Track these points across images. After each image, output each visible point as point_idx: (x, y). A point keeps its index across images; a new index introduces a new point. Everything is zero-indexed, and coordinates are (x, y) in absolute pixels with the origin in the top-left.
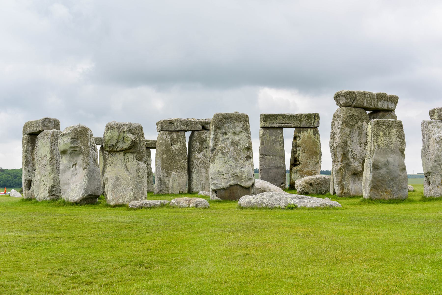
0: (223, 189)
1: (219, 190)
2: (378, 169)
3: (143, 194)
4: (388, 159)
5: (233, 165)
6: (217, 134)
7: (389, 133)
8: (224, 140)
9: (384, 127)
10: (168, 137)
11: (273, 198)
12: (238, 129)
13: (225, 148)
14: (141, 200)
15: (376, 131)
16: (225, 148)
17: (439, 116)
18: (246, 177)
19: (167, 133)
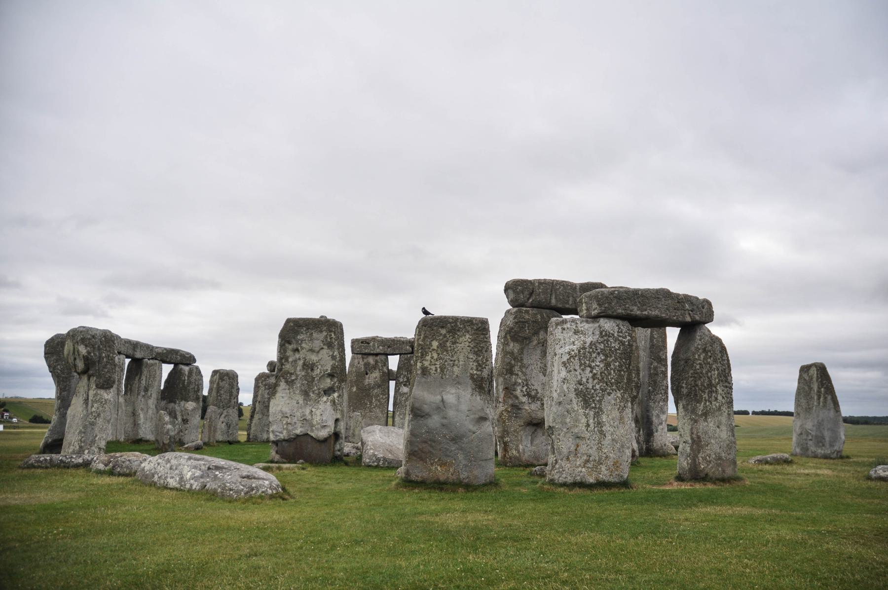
0: (284, 440)
1: (278, 441)
2: (422, 417)
3: (93, 442)
4: (445, 397)
5: (301, 402)
6: (285, 351)
7: (454, 343)
8: (295, 361)
9: (443, 331)
10: (362, 363)
11: (168, 465)
12: (317, 344)
13: (291, 374)
14: (89, 452)
15: (424, 340)
16: (291, 374)
17: (587, 309)
18: (318, 424)
19: (360, 356)
